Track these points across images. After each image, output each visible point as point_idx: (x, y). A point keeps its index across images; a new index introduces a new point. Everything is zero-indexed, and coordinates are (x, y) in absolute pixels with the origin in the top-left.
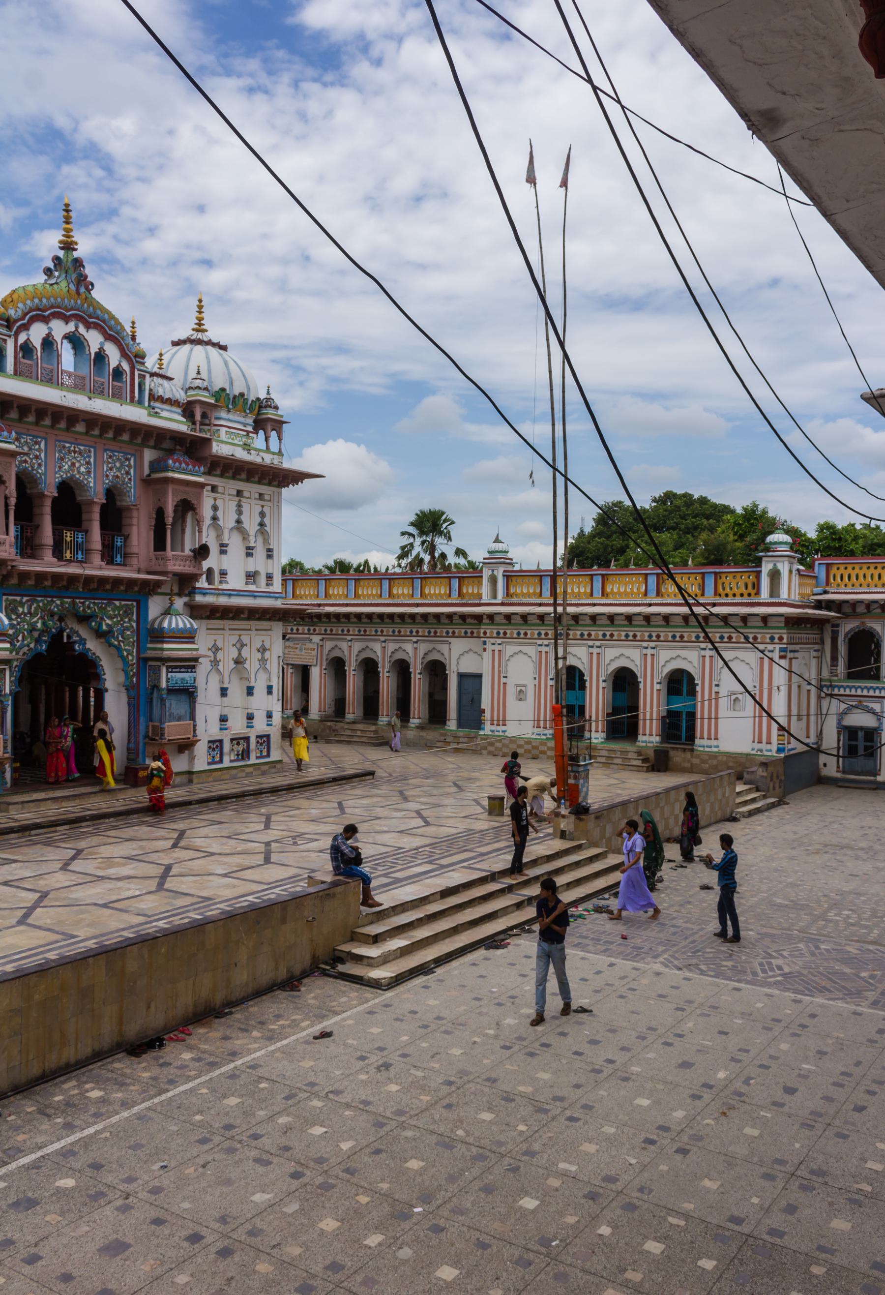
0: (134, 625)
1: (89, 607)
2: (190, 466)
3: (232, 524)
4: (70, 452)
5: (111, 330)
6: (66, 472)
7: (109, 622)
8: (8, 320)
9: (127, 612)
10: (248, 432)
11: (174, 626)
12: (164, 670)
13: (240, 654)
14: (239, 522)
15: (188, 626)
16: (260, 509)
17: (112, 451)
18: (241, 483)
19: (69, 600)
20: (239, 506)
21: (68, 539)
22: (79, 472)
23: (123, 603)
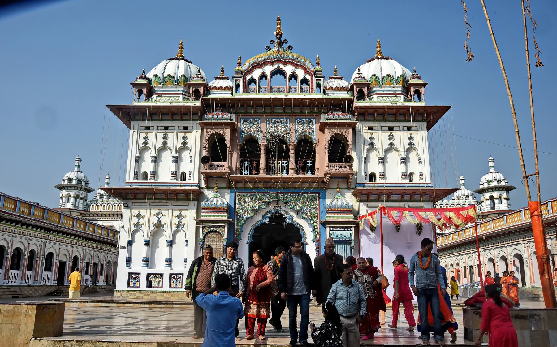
0: (317, 206)
1: (287, 198)
2: (341, 116)
8: (242, 72)
9: (313, 199)
10: (396, 95)
11: (334, 203)
12: (328, 229)
14: (391, 144)
15: (345, 203)
16: (409, 136)
18: (391, 123)
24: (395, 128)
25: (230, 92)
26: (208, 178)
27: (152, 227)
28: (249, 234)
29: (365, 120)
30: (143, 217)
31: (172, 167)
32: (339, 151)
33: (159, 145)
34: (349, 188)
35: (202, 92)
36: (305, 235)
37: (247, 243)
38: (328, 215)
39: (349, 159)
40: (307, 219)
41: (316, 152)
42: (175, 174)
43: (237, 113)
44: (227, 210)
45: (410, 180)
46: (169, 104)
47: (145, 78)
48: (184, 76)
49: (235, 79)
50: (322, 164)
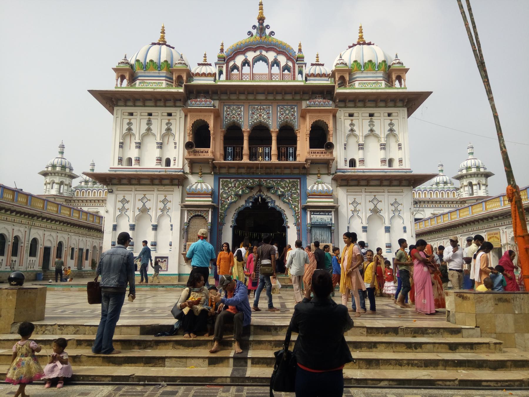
0: (299, 191)
1: (269, 183)
3: (366, 132)
4: (257, 110)
5: (281, 49)
6: (256, 119)
7: (283, 190)
8: (224, 58)
11: (315, 188)
12: (309, 213)
13: (375, 206)
14: (372, 130)
15: (326, 188)
17: (282, 106)
19: (257, 180)
20: (371, 121)
21: (260, 151)
22: (264, 119)
23: (291, 180)
24: (375, 115)
25: (213, 78)
26: (192, 163)
27: (137, 213)
28: (233, 218)
29: (345, 107)
30: (128, 202)
31: (157, 153)
32: (320, 137)
33: (143, 131)
34: (329, 174)
35: (185, 78)
36: (287, 219)
37: (231, 227)
38: (308, 200)
39: (330, 146)
40: (289, 203)
41: (298, 139)
42: (159, 160)
43: (219, 99)
44: (211, 195)
45: (390, 165)
46: (152, 90)
47: (128, 63)
48: (166, 61)
49: (217, 66)
50: (303, 150)
